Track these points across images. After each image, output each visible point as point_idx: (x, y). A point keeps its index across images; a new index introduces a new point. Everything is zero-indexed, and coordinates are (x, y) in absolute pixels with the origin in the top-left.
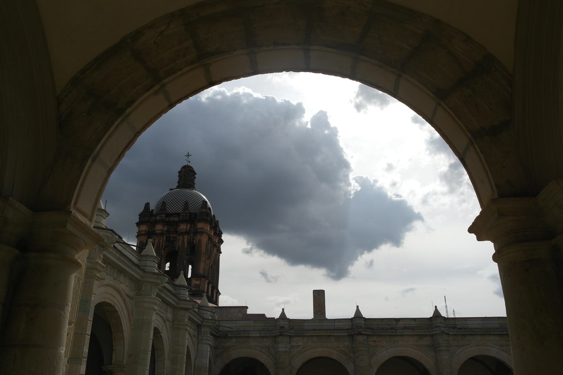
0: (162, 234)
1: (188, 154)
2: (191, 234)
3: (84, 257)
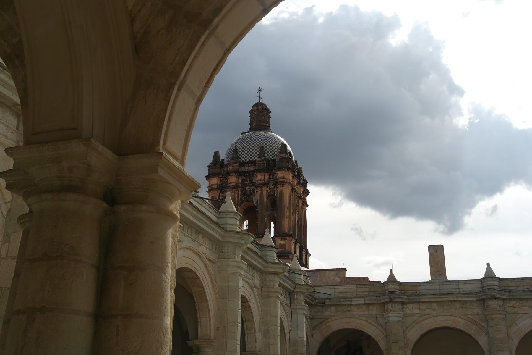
0: (236, 187)
1: (259, 88)
2: (271, 185)
3: (176, 210)
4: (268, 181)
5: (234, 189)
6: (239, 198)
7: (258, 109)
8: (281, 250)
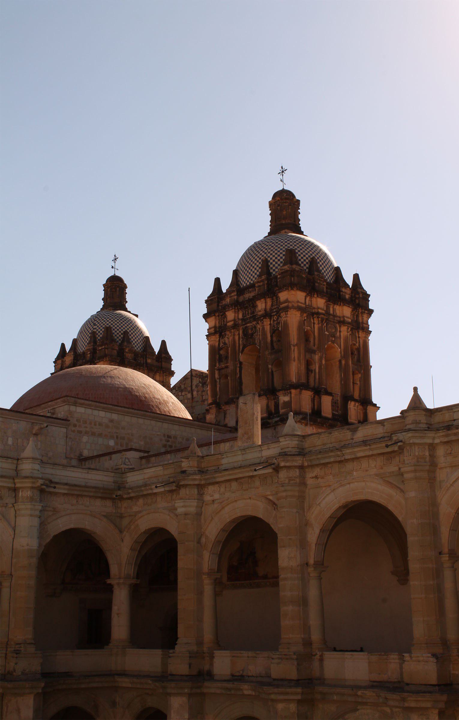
0: (235, 326)
1: (282, 168)
4: (271, 310)
5: (232, 330)
6: (241, 342)
7: (275, 202)
8: (285, 410)
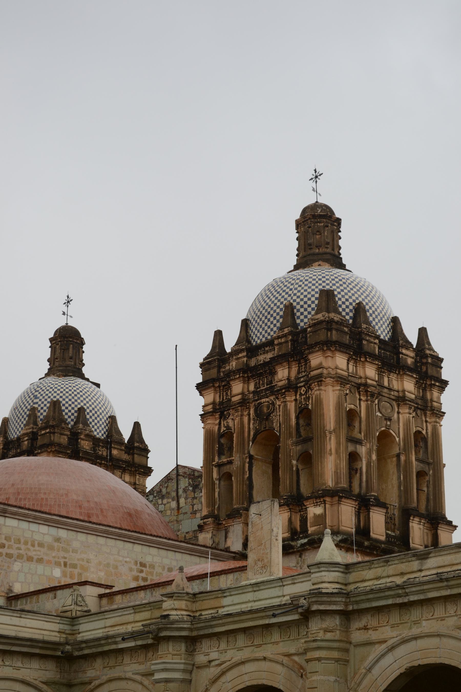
0: (244, 403)
1: (316, 172)
2: (302, 386)
4: (297, 379)
5: (239, 408)
7: (305, 221)
8: (316, 527)
